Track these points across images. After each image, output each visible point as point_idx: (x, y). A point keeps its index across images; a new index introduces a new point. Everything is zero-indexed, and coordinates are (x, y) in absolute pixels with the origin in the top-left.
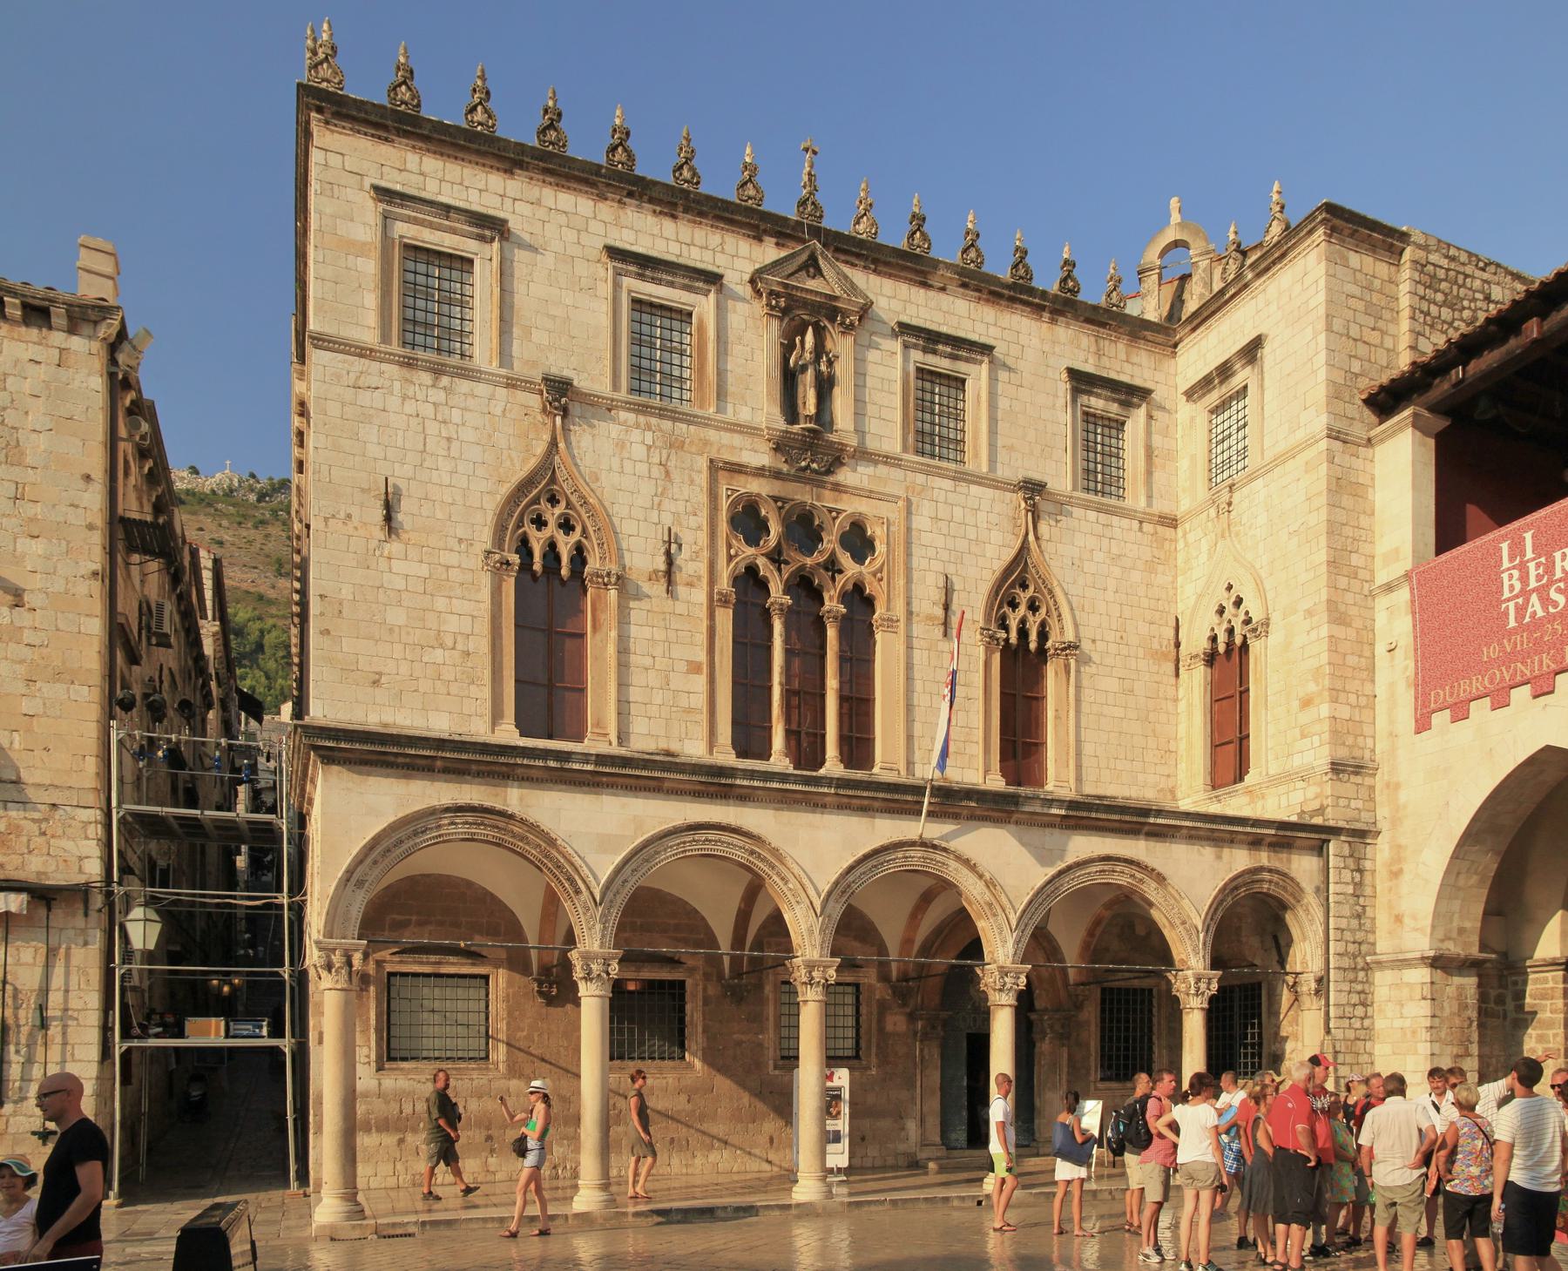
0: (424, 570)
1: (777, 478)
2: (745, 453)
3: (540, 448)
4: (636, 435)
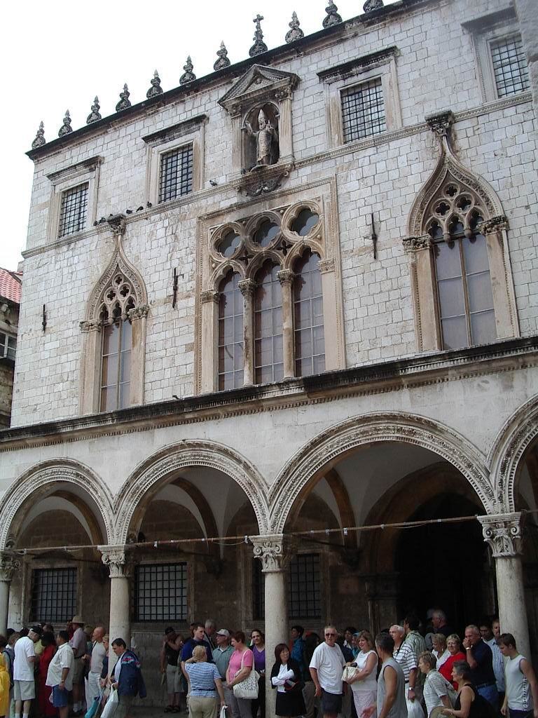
0: (57, 344)
1: (240, 208)
3: (110, 255)
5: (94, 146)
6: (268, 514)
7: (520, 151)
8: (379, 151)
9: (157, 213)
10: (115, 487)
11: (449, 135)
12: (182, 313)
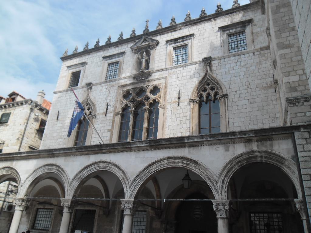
3: (85, 96)
4: (104, 87)
5: (85, 58)
6: (129, 191)
9: (104, 83)
10: (71, 176)
11: (210, 64)
12: (108, 118)
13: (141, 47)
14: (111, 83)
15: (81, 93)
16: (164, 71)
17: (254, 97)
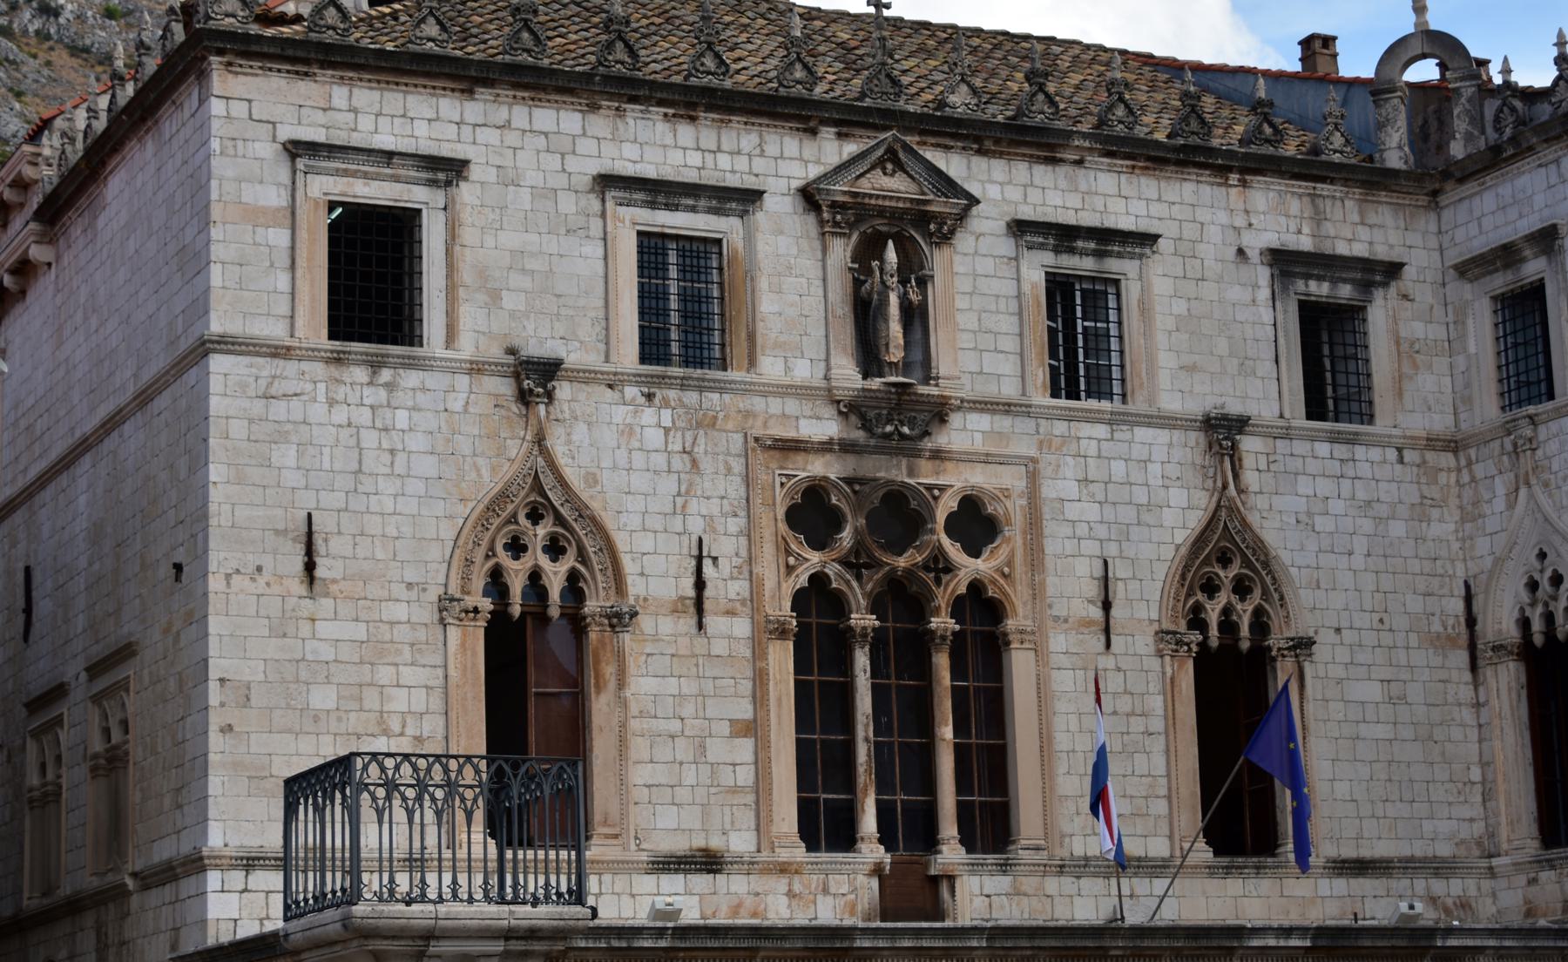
0: (360, 632)
2: (802, 422)
4: (648, 415)
7: (1332, 529)
8: (1117, 435)
13: (873, 202)
14: (691, 397)
15: (466, 411)
16: (1017, 414)
17: (1403, 677)
